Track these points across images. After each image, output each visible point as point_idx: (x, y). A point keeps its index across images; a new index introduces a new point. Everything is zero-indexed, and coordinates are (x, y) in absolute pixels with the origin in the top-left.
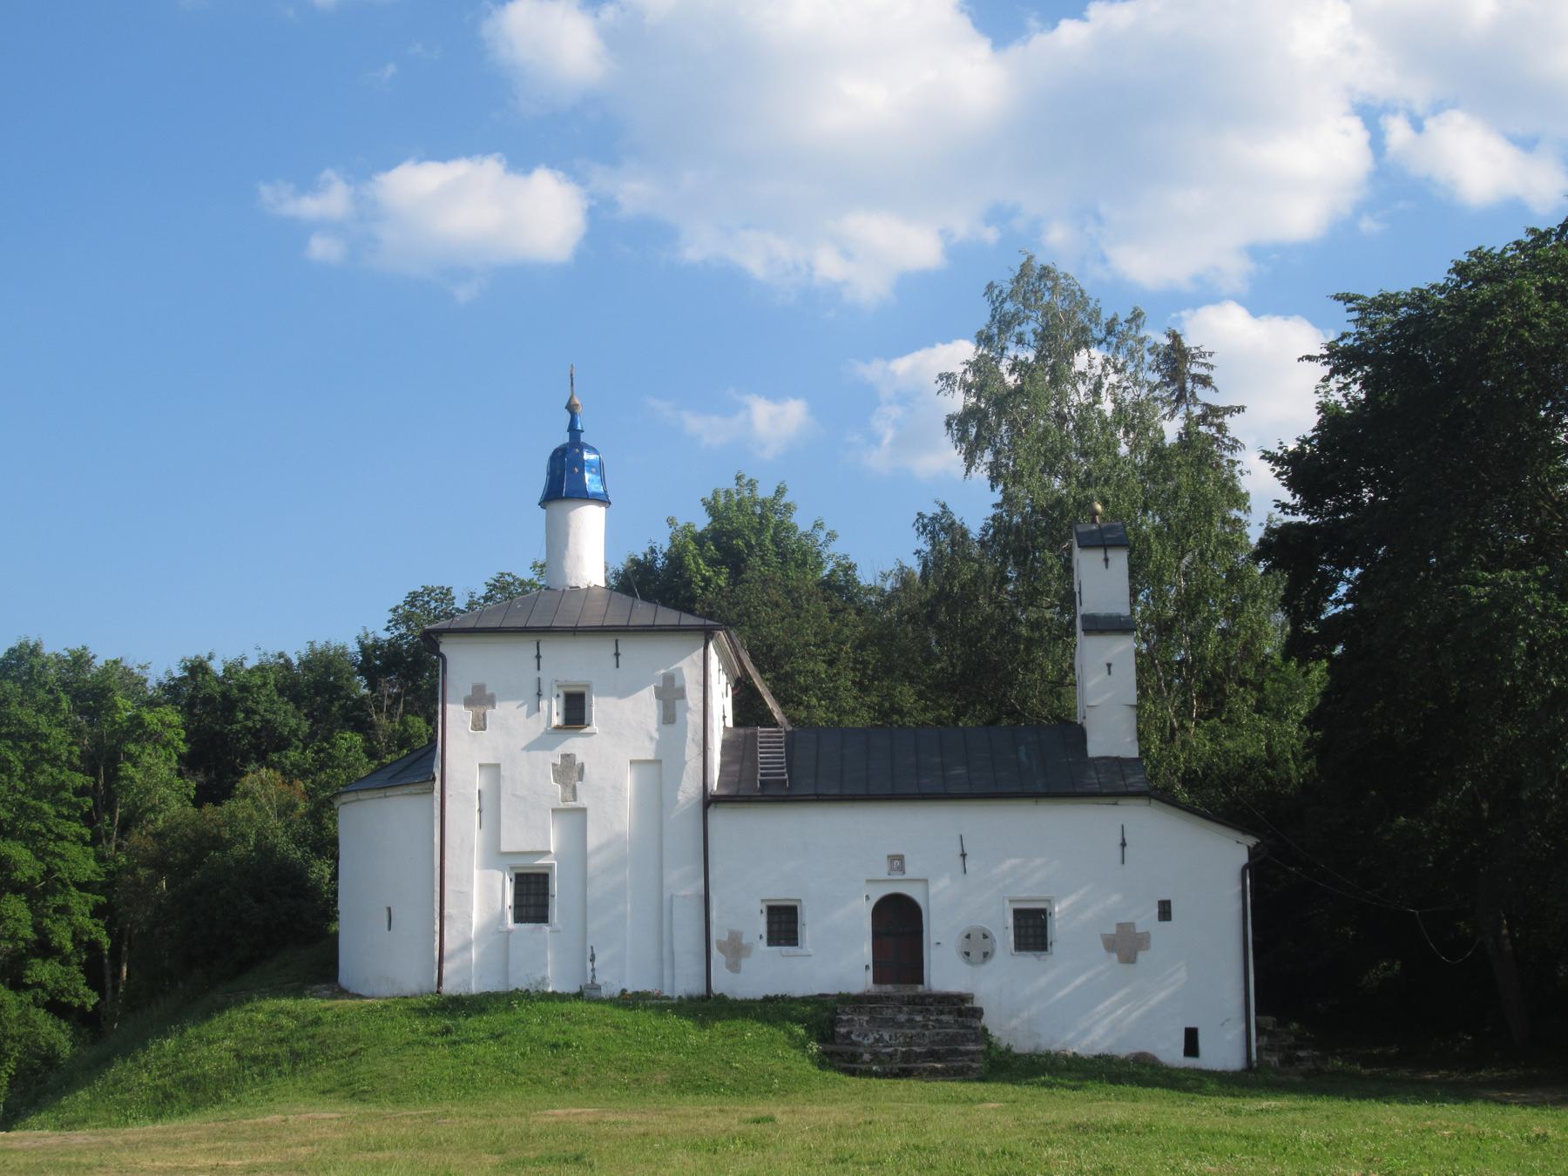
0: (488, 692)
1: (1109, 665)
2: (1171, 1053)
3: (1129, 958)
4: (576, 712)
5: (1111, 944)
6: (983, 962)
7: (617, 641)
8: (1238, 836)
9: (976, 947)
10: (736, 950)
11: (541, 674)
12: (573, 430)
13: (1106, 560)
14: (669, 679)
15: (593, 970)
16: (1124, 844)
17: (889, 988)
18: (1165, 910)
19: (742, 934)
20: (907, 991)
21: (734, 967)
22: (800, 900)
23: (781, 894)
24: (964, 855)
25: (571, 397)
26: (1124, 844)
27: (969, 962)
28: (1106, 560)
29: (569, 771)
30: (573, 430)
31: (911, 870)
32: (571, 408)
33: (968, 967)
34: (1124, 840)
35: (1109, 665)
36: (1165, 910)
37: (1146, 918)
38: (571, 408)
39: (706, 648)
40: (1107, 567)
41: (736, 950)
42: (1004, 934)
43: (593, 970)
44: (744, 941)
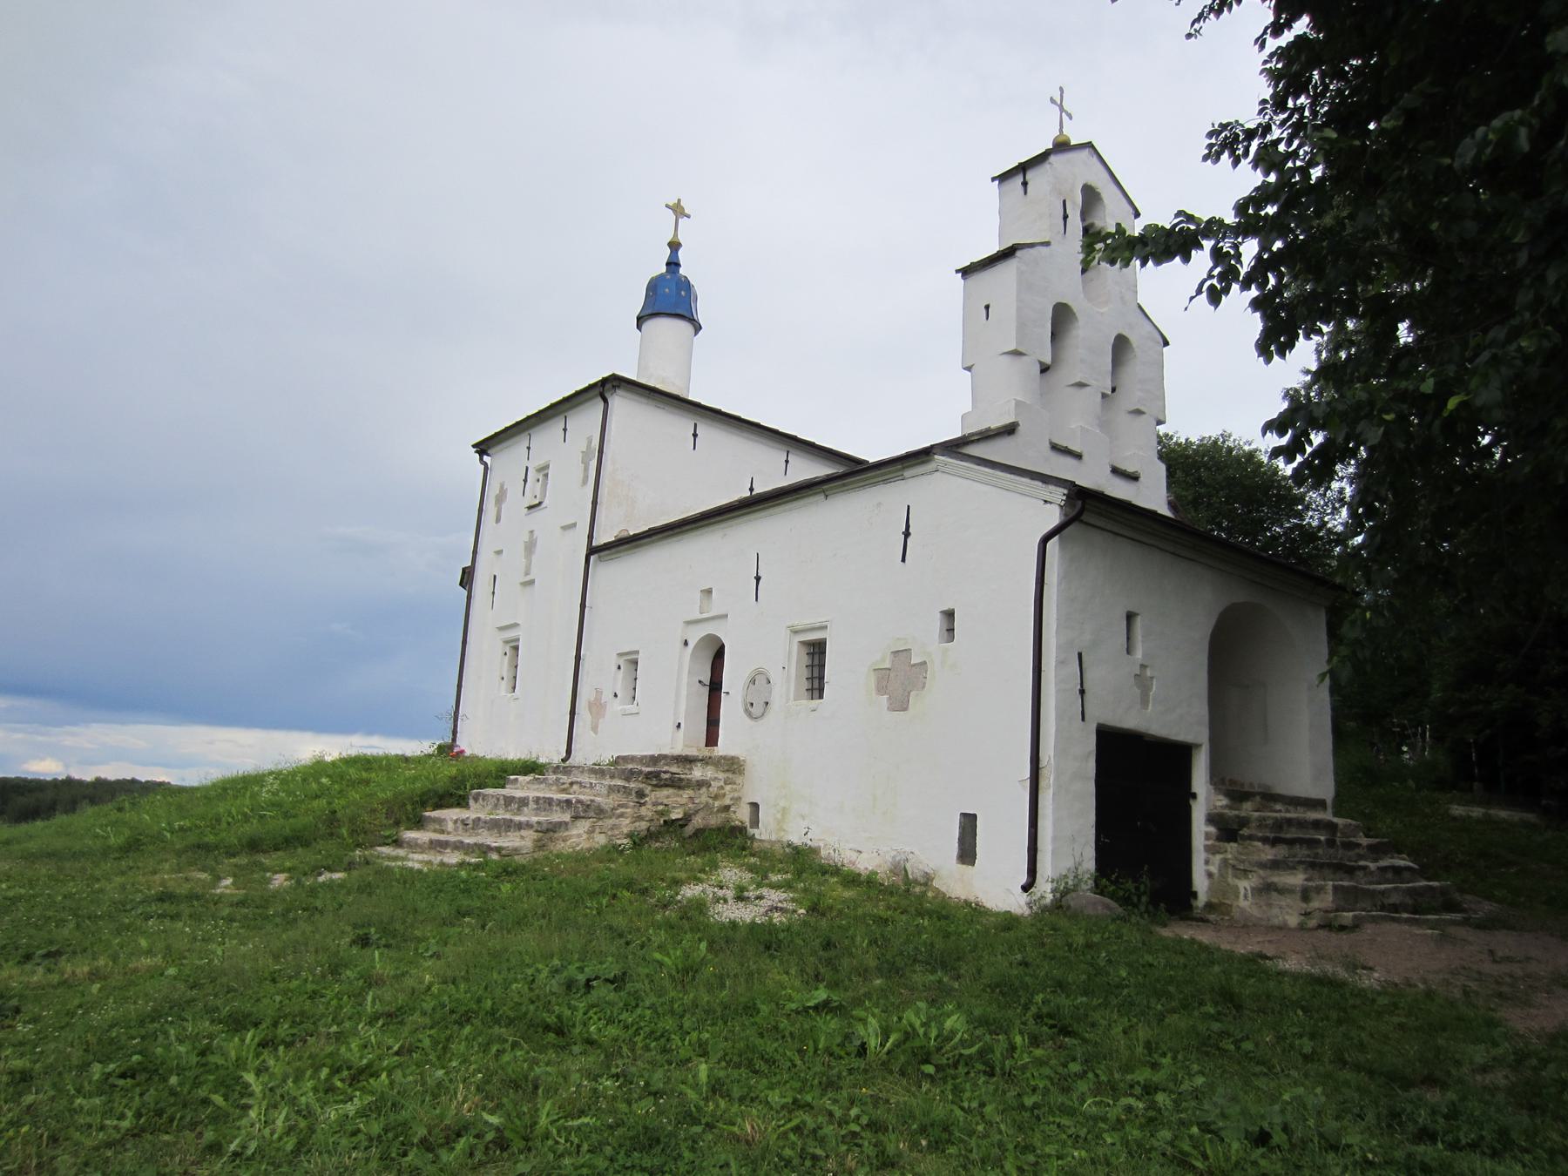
1: (987, 307)
12: (673, 264)
13: (1025, 184)
22: (637, 652)
24: (758, 579)
26: (907, 534)
27: (749, 715)
28: (1025, 184)
30: (673, 264)
32: (675, 246)
33: (752, 723)
35: (987, 307)
38: (675, 246)
39: (605, 401)
40: (1026, 193)
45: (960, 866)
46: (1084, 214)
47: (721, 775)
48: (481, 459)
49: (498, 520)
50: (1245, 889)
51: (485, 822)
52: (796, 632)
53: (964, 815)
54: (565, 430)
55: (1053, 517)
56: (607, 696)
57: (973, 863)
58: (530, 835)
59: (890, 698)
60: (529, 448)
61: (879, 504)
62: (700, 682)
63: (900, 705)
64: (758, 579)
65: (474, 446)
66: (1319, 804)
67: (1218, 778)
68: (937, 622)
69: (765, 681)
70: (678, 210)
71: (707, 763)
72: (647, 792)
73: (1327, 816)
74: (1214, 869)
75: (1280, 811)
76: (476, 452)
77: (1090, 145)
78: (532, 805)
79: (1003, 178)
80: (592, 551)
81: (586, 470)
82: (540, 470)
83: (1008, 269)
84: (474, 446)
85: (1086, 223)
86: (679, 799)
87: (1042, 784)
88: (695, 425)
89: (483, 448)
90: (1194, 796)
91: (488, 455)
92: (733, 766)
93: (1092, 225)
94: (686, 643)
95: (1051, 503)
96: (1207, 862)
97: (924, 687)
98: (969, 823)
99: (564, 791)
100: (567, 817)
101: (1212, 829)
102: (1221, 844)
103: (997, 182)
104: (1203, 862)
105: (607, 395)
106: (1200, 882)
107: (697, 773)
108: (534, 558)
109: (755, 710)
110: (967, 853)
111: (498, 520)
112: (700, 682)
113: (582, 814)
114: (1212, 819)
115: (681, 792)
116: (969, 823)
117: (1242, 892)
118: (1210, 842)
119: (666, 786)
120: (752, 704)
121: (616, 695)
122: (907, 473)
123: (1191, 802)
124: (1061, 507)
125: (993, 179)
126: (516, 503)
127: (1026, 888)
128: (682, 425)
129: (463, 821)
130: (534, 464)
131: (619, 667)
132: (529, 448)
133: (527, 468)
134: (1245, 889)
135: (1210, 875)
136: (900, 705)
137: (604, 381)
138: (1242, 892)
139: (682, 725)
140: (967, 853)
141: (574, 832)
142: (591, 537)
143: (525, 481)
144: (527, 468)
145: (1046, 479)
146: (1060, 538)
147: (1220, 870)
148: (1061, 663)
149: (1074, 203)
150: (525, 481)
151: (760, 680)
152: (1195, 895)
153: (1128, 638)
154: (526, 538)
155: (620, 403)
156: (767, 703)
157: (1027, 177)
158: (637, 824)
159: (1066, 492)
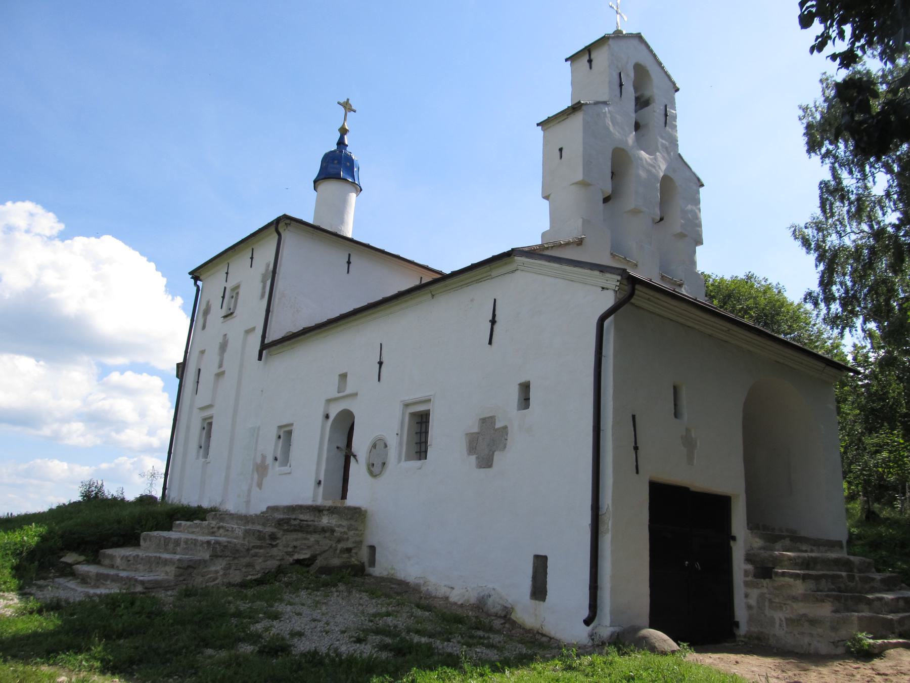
1: (561, 150)
7: (253, 249)
12: (341, 143)
13: (590, 61)
16: (493, 322)
24: (381, 363)
26: (493, 322)
28: (590, 61)
30: (341, 143)
32: (343, 131)
34: (494, 315)
35: (561, 150)
38: (343, 131)
40: (591, 68)
45: (533, 601)
46: (636, 88)
47: (345, 523)
48: (195, 283)
49: (204, 327)
50: (780, 620)
51: (142, 559)
52: (407, 405)
53: (537, 557)
54: (252, 258)
55: (608, 300)
56: (269, 460)
58: (171, 570)
59: (477, 458)
60: (227, 273)
61: (472, 300)
62: (338, 448)
63: (486, 462)
64: (381, 363)
65: (190, 273)
66: (834, 545)
67: (753, 525)
68: (514, 394)
69: (383, 446)
70: (347, 106)
71: (333, 513)
72: (279, 535)
73: (842, 554)
74: (753, 602)
75: (806, 551)
76: (192, 278)
77: (639, 37)
78: (183, 545)
79: (572, 59)
80: (264, 346)
81: (264, 287)
82: (233, 290)
83: (578, 120)
84: (190, 273)
85: (638, 94)
86: (306, 542)
87: (602, 529)
88: (349, 255)
89: (196, 275)
90: (734, 538)
91: (200, 280)
92: (357, 514)
93: (642, 96)
94: (327, 417)
95: (607, 289)
96: (746, 596)
97: (505, 447)
98: (541, 563)
99: (213, 534)
100: (206, 556)
101: (750, 567)
102: (759, 580)
103: (569, 63)
104: (743, 595)
105: (281, 230)
106: (741, 613)
107: (325, 521)
108: (226, 355)
109: (375, 469)
110: (539, 591)
111: (204, 327)
112: (338, 448)
113: (219, 554)
114: (749, 559)
115: (309, 536)
116: (541, 563)
117: (778, 622)
118: (750, 578)
119: (295, 530)
120: (373, 465)
121: (276, 459)
122: (494, 273)
123: (732, 543)
124: (616, 292)
125: (567, 60)
126: (217, 312)
127: (587, 622)
128: (338, 257)
130: (230, 285)
131: (279, 437)
132: (227, 273)
133: (225, 288)
134: (780, 620)
135: (749, 607)
136: (486, 462)
137: (278, 221)
138: (778, 622)
139: (322, 483)
140: (539, 591)
141: (213, 569)
142: (264, 337)
143: (223, 297)
144: (225, 288)
145: (602, 269)
146: (615, 320)
147: (758, 602)
148: (616, 424)
149: (628, 75)
150: (223, 297)
151: (380, 446)
152: (737, 624)
153: (675, 405)
154: (220, 340)
155: (290, 237)
156: (384, 464)
157: (592, 57)
158: (269, 563)
159: (619, 278)
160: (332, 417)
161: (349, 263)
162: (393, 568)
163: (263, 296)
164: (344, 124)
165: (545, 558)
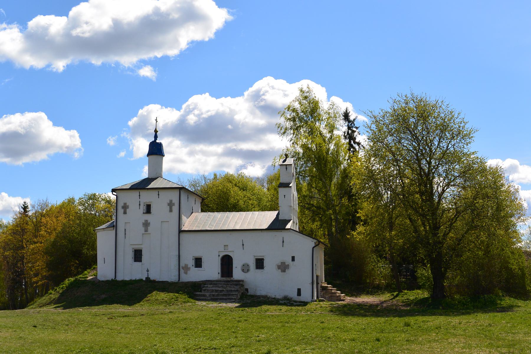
0: (127, 205)
1: (285, 196)
2: (293, 294)
3: (284, 271)
4: (148, 209)
5: (279, 267)
6: (247, 272)
8: (312, 239)
9: (245, 269)
10: (186, 269)
11: (140, 200)
12: (156, 137)
13: (286, 168)
14: (171, 201)
15: (148, 274)
16: (283, 242)
17: (224, 279)
18: (293, 259)
19: (188, 265)
20: (228, 279)
21: (186, 273)
23: (198, 255)
24: (243, 245)
25: (156, 128)
26: (283, 242)
28: (286, 168)
29: (146, 224)
31: (230, 248)
35: (285, 196)
36: (293, 259)
37: (288, 261)
41: (186, 269)
42: (252, 265)
43: (148, 274)
44: (189, 267)
49: (125, 213)
54: (159, 195)
57: (300, 296)
64: (243, 245)
74: (322, 294)
98: (299, 291)
101: (321, 288)
111: (125, 213)
116: (299, 291)
129: (213, 295)
143: (140, 205)
150: (140, 205)
156: (248, 270)
160: (221, 256)
161: (188, 198)
162: (255, 293)
163: (171, 211)
164: (156, 128)
165: (300, 289)
